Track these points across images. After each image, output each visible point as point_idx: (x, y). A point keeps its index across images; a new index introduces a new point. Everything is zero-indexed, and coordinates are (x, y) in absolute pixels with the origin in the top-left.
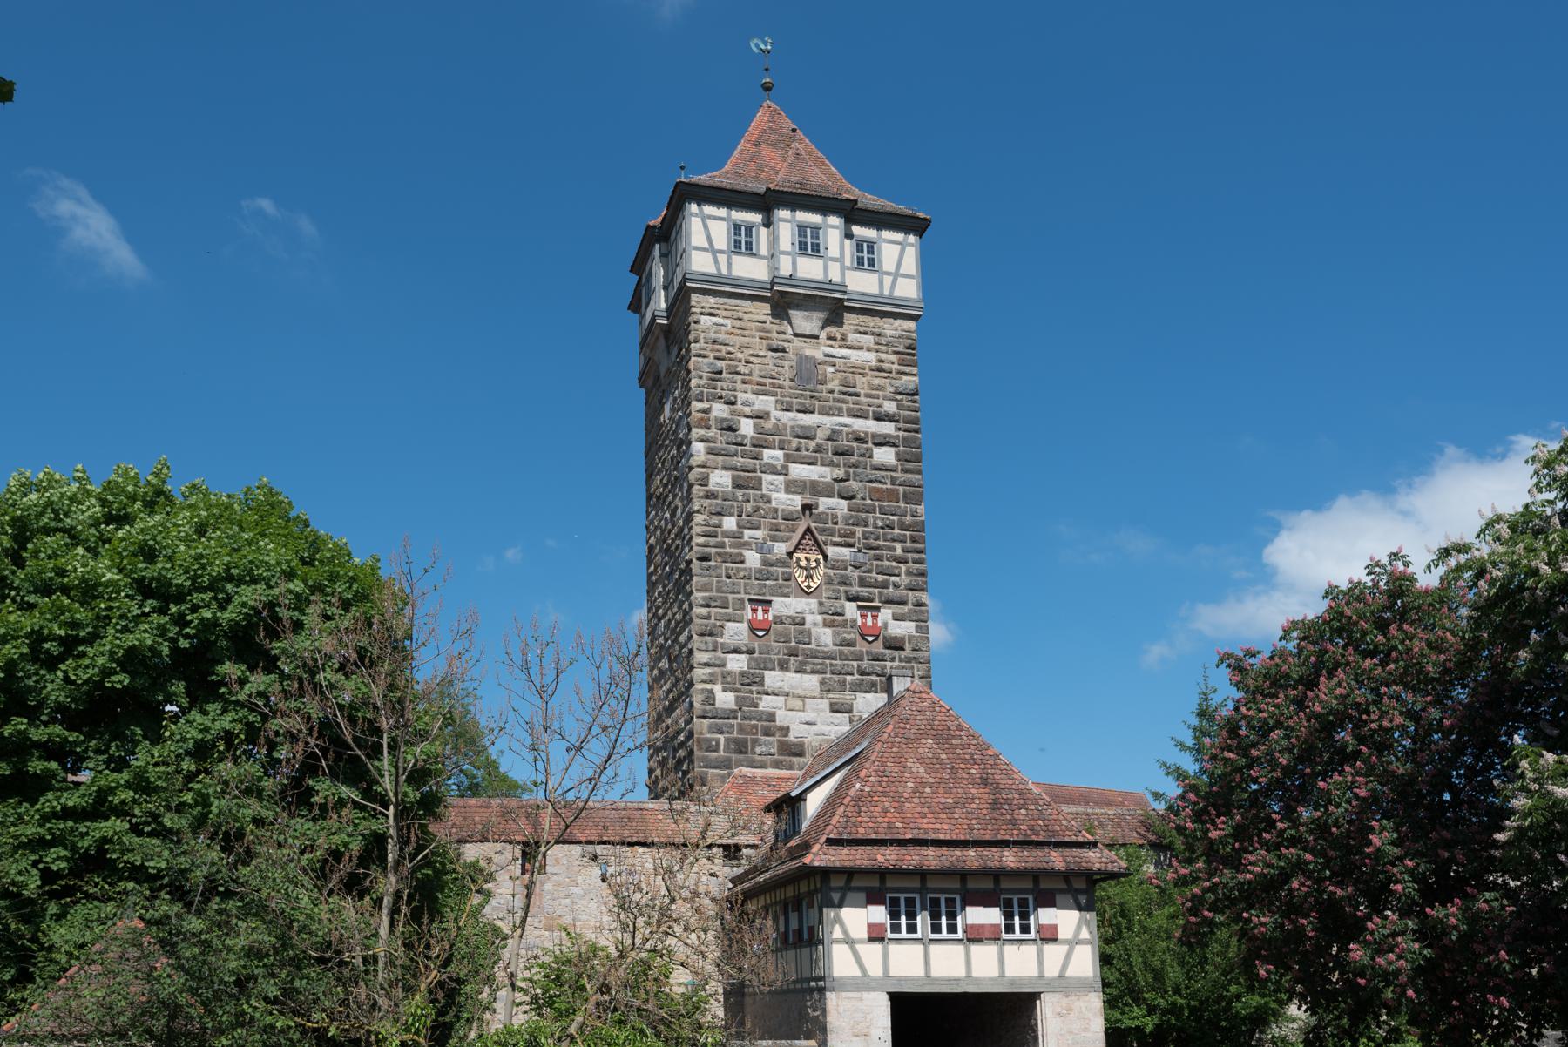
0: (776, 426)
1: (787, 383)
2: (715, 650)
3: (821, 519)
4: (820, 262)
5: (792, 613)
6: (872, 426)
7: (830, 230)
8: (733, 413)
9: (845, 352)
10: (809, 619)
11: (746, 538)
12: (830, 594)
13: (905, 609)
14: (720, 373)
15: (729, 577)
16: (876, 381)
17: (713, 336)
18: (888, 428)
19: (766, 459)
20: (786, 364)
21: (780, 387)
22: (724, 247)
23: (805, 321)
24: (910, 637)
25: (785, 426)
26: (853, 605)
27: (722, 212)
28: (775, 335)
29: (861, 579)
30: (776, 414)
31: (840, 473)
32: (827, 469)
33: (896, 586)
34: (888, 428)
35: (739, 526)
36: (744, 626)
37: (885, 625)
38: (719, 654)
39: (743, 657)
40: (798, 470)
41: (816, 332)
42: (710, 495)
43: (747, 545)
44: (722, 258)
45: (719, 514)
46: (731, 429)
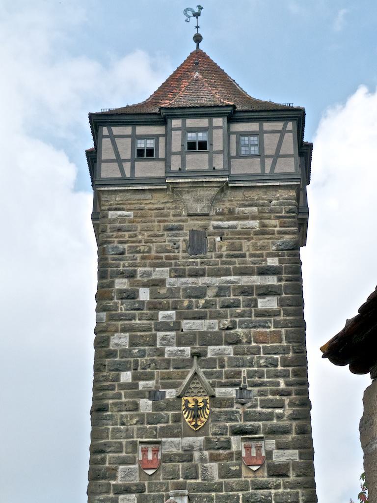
0: (170, 290)
1: (181, 254)
2: (108, 492)
3: (211, 363)
4: (205, 157)
5: (180, 451)
6: (256, 280)
7: (215, 131)
8: (131, 285)
9: (232, 223)
10: (196, 455)
11: (140, 388)
12: (215, 430)
13: (290, 438)
14: (123, 253)
15: (123, 424)
16: (260, 243)
17: (118, 225)
18: (271, 280)
19: (160, 319)
20: (182, 239)
21: (175, 258)
22: (129, 157)
23: (195, 202)
24: (295, 465)
25: (179, 288)
26: (239, 437)
27: (128, 130)
28: (172, 218)
29: (246, 414)
30: (170, 281)
31: (226, 322)
32: (216, 321)
33: (280, 417)
34: (271, 280)
35: (136, 378)
36: (137, 466)
37: (269, 454)
38: (111, 495)
39: (134, 495)
40: (187, 325)
41: (206, 211)
42: (112, 354)
43: (141, 395)
44: (127, 166)
45: (117, 370)
46: (128, 298)
